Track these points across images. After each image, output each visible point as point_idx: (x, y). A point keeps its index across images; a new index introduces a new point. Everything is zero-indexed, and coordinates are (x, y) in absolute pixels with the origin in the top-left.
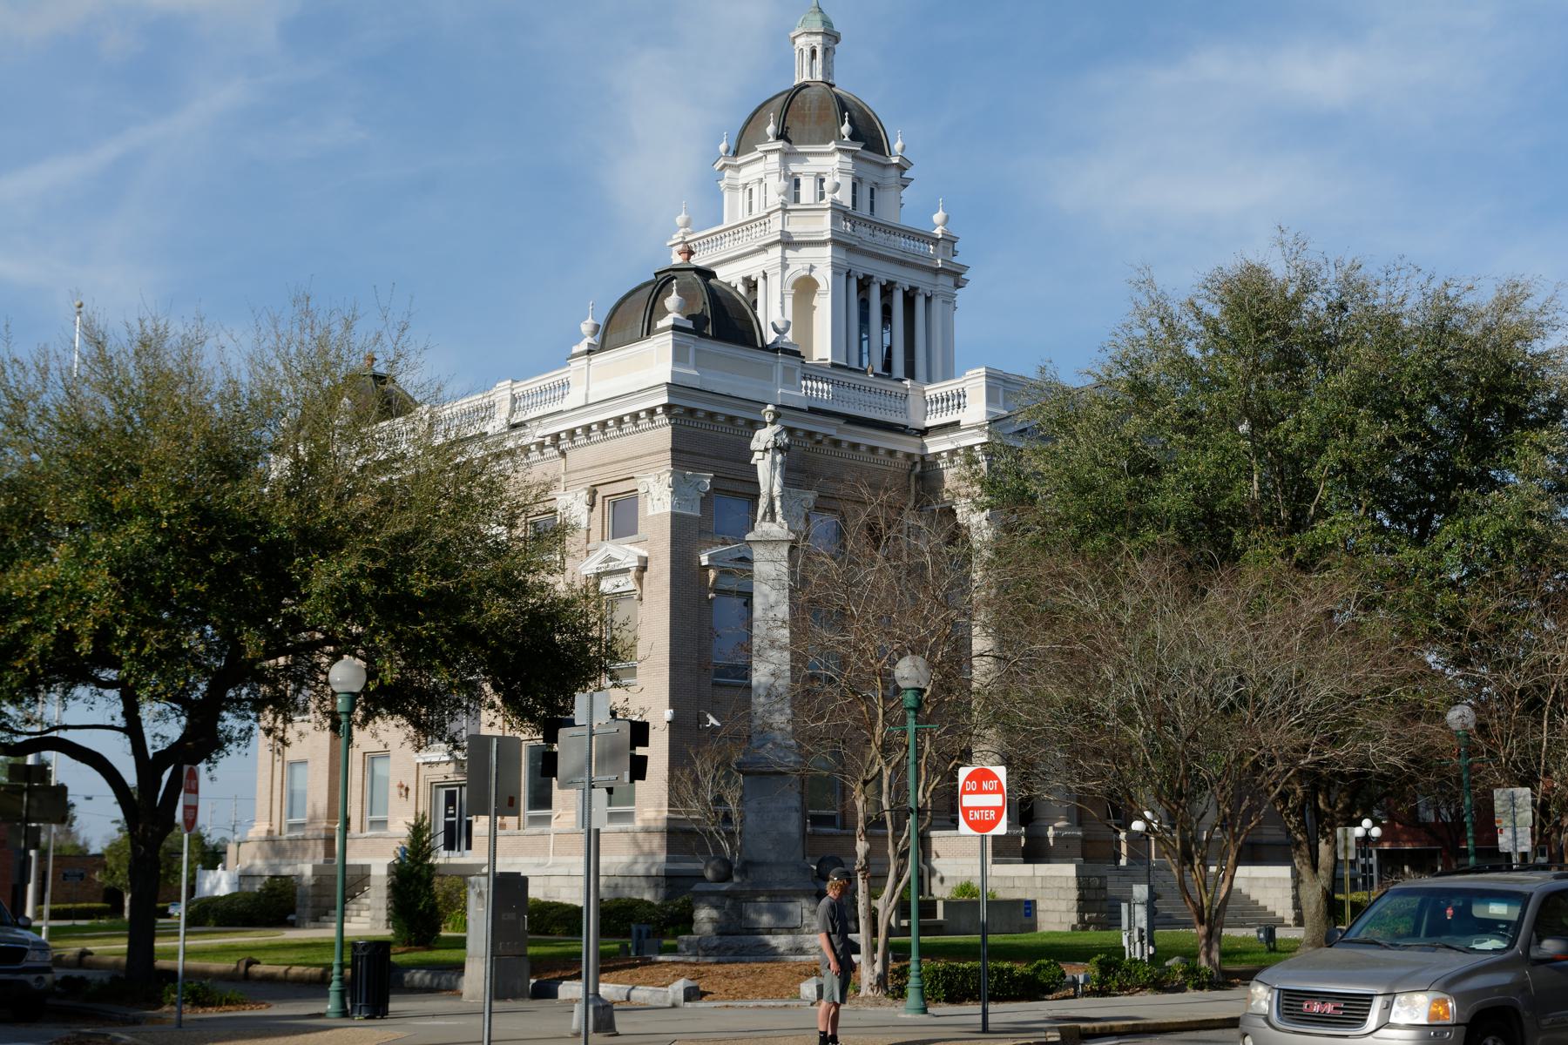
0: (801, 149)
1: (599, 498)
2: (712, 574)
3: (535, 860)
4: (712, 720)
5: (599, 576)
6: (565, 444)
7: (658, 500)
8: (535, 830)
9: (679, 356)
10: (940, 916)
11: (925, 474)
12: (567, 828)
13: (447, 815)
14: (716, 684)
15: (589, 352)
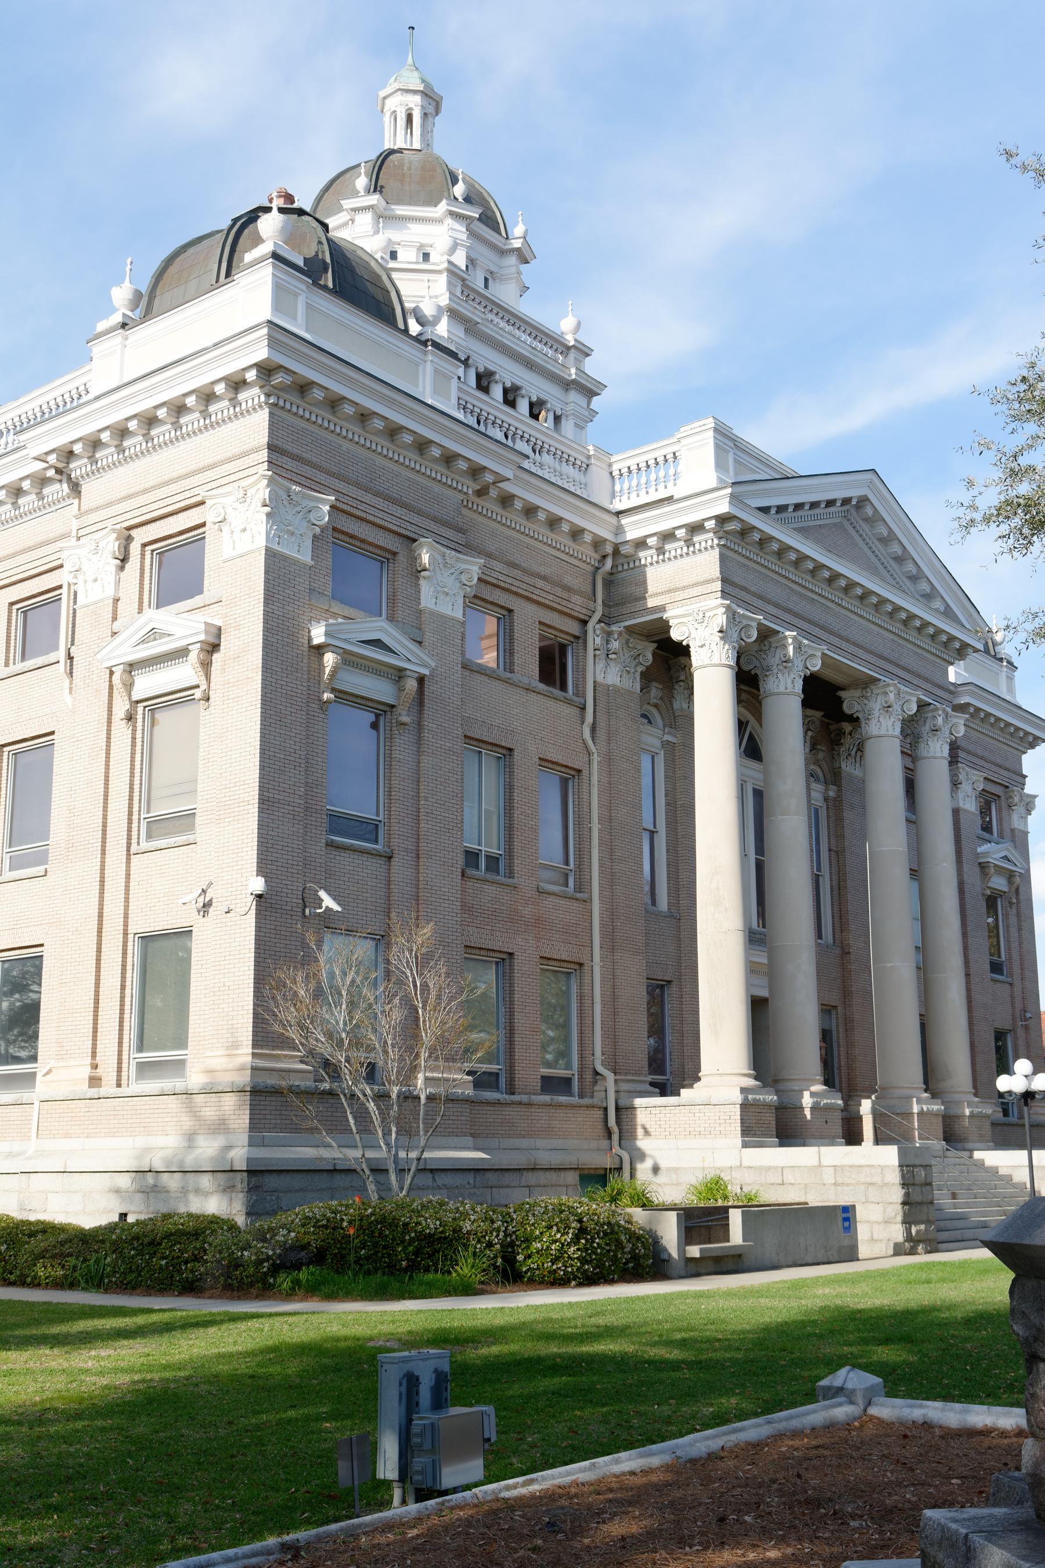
0: (401, 210)
1: (135, 548)
2: (330, 659)
4: (328, 902)
5: (131, 667)
6: (78, 468)
7: (241, 533)
10: (736, 1235)
11: (616, 573)
14: (330, 845)
15: (124, 325)
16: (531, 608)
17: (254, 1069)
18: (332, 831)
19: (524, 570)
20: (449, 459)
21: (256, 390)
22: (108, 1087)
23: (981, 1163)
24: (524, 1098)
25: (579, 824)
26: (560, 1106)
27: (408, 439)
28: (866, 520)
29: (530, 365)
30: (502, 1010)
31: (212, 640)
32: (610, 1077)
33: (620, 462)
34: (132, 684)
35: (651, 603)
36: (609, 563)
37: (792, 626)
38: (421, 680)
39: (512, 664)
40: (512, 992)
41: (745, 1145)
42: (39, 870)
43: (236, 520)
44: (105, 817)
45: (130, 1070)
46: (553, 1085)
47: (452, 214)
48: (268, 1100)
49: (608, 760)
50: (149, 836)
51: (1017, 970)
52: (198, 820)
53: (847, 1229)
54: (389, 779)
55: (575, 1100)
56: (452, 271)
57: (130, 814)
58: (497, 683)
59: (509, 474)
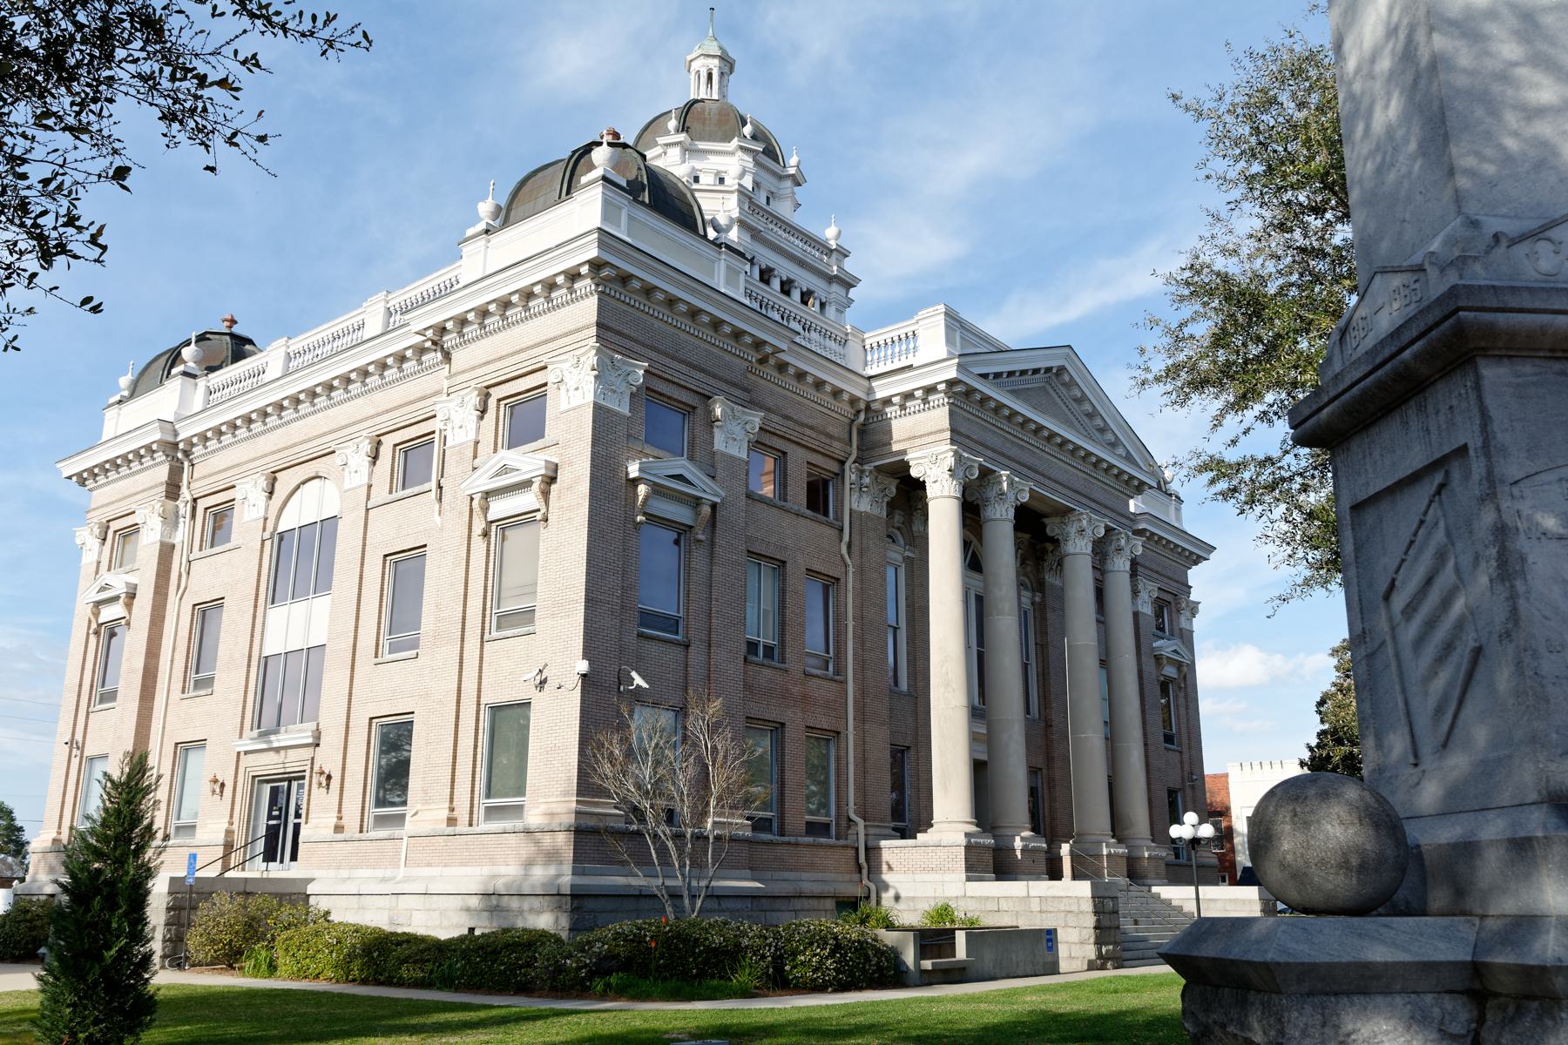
0: (702, 145)
1: (492, 403)
2: (642, 489)
3: (380, 873)
4: (638, 681)
5: (487, 495)
6: (449, 340)
7: (575, 394)
8: (383, 833)
9: (608, 209)
10: (961, 952)
11: (868, 424)
12: (426, 828)
13: (270, 817)
14: (641, 635)
15: (487, 232)
16: (800, 452)
17: (578, 813)
18: (642, 625)
19: (796, 422)
20: (738, 334)
21: (588, 281)
22: (462, 827)
23: (1157, 897)
24: (792, 839)
25: (837, 621)
26: (821, 845)
27: (706, 319)
28: (1064, 384)
29: (801, 263)
30: (775, 768)
31: (550, 474)
32: (861, 823)
33: (871, 338)
34: (487, 509)
35: (895, 448)
36: (862, 417)
37: (1006, 467)
38: (714, 506)
39: (786, 494)
40: (783, 755)
41: (969, 879)
42: (412, 653)
43: (571, 381)
44: (464, 612)
45: (480, 813)
46: (814, 829)
47: (741, 148)
48: (589, 837)
49: (861, 572)
50: (499, 628)
51: (1185, 741)
52: (537, 614)
53: (1050, 949)
54: (687, 583)
55: (832, 841)
56: (741, 191)
57: (484, 609)
58: (774, 510)
59: (784, 347)
